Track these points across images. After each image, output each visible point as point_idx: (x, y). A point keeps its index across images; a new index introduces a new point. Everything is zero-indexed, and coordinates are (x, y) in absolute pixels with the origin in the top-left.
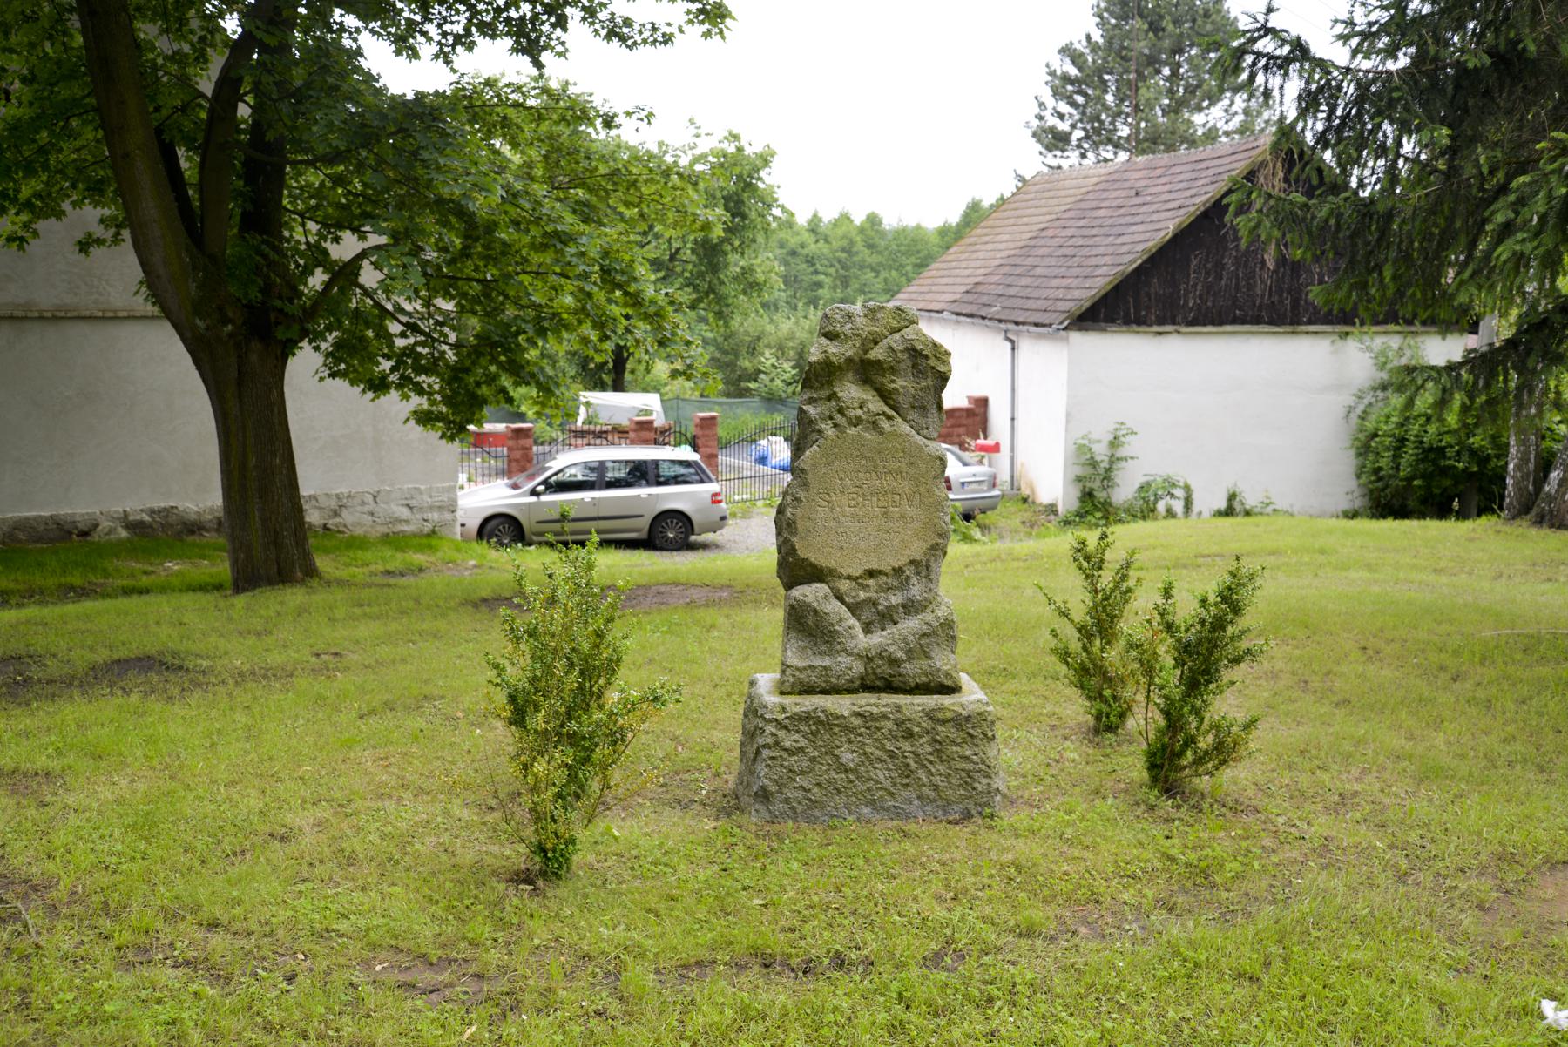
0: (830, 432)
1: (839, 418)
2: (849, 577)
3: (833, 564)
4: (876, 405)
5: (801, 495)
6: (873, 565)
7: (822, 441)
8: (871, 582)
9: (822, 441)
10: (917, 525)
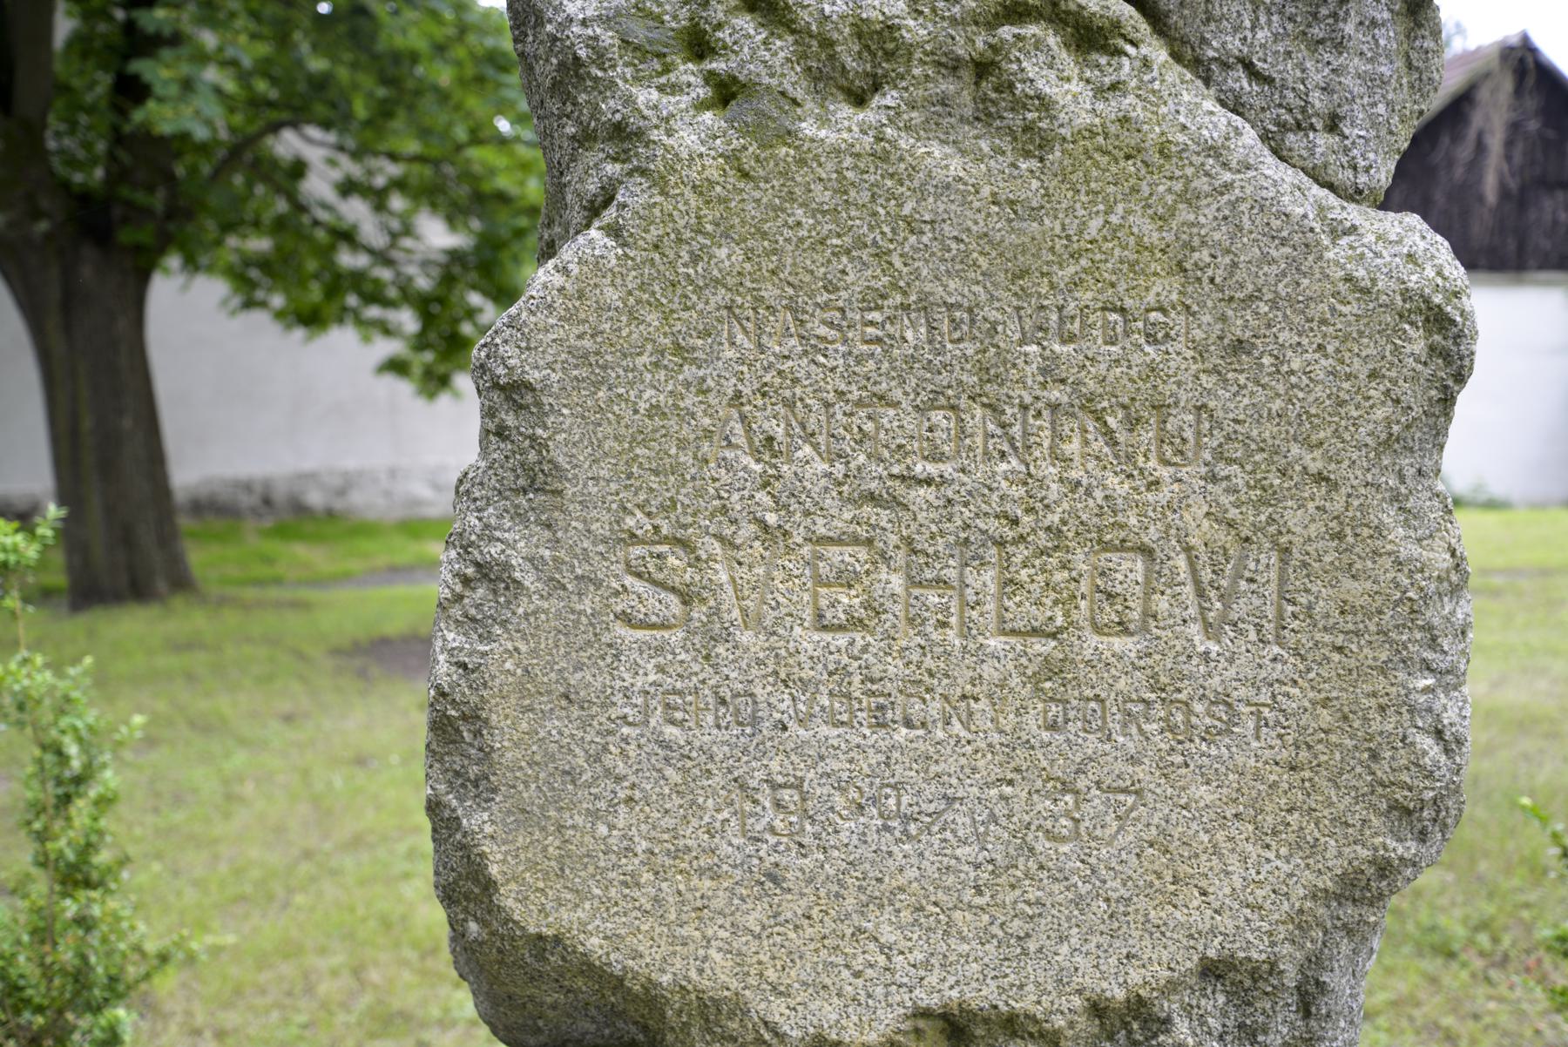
0: (690, 131)
3: (718, 974)
5: (516, 546)
9: (634, 195)
10: (1254, 749)
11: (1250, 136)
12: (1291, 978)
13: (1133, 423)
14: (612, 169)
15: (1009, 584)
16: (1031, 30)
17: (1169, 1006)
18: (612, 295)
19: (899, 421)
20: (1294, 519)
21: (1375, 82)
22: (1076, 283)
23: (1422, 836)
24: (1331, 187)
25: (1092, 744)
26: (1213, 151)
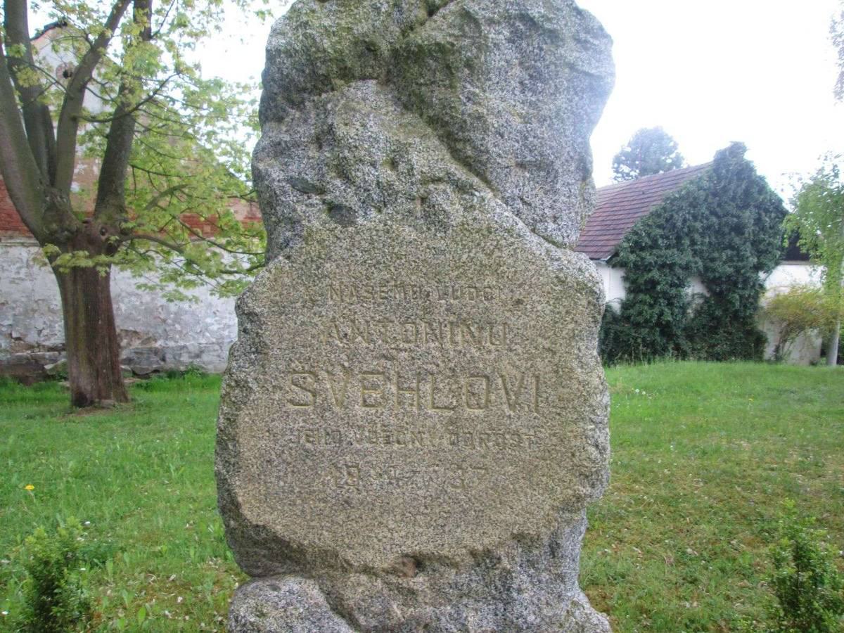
1: (338, 189)
2: (367, 570)
4: (428, 155)
5: (249, 374)
6: (423, 543)
7: (297, 244)
8: (419, 582)
9: (297, 244)
11: (521, 224)
12: (546, 541)
13: (481, 329)
14: (288, 234)
15: (436, 389)
16: (441, 186)
17: (501, 552)
18: (287, 281)
19: (395, 329)
20: (540, 365)
21: (570, 207)
22: (458, 277)
23: (593, 486)
24: (554, 243)
25: (468, 451)
26: (508, 231)
